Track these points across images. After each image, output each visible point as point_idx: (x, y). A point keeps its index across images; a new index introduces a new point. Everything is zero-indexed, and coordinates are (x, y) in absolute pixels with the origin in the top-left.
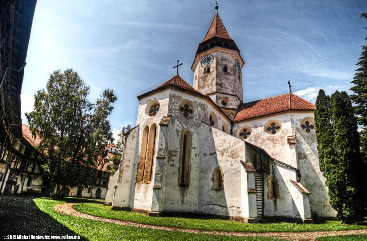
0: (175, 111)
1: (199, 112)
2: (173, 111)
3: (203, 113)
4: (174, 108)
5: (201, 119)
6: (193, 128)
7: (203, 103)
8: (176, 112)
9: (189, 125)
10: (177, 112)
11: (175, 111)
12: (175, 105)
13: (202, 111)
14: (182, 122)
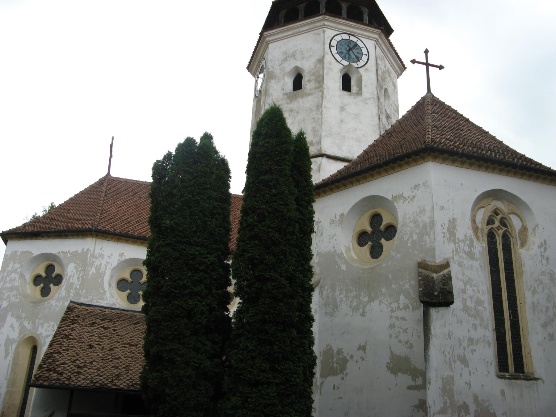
0: (9, 293)
1: (70, 276)
2: (4, 294)
3: (78, 278)
4: (9, 285)
5: (72, 295)
6: (46, 325)
7: (83, 249)
8: (12, 293)
9: (37, 321)
10: (13, 295)
11: (9, 293)
12: (13, 278)
13: (77, 271)
14: (24, 315)
